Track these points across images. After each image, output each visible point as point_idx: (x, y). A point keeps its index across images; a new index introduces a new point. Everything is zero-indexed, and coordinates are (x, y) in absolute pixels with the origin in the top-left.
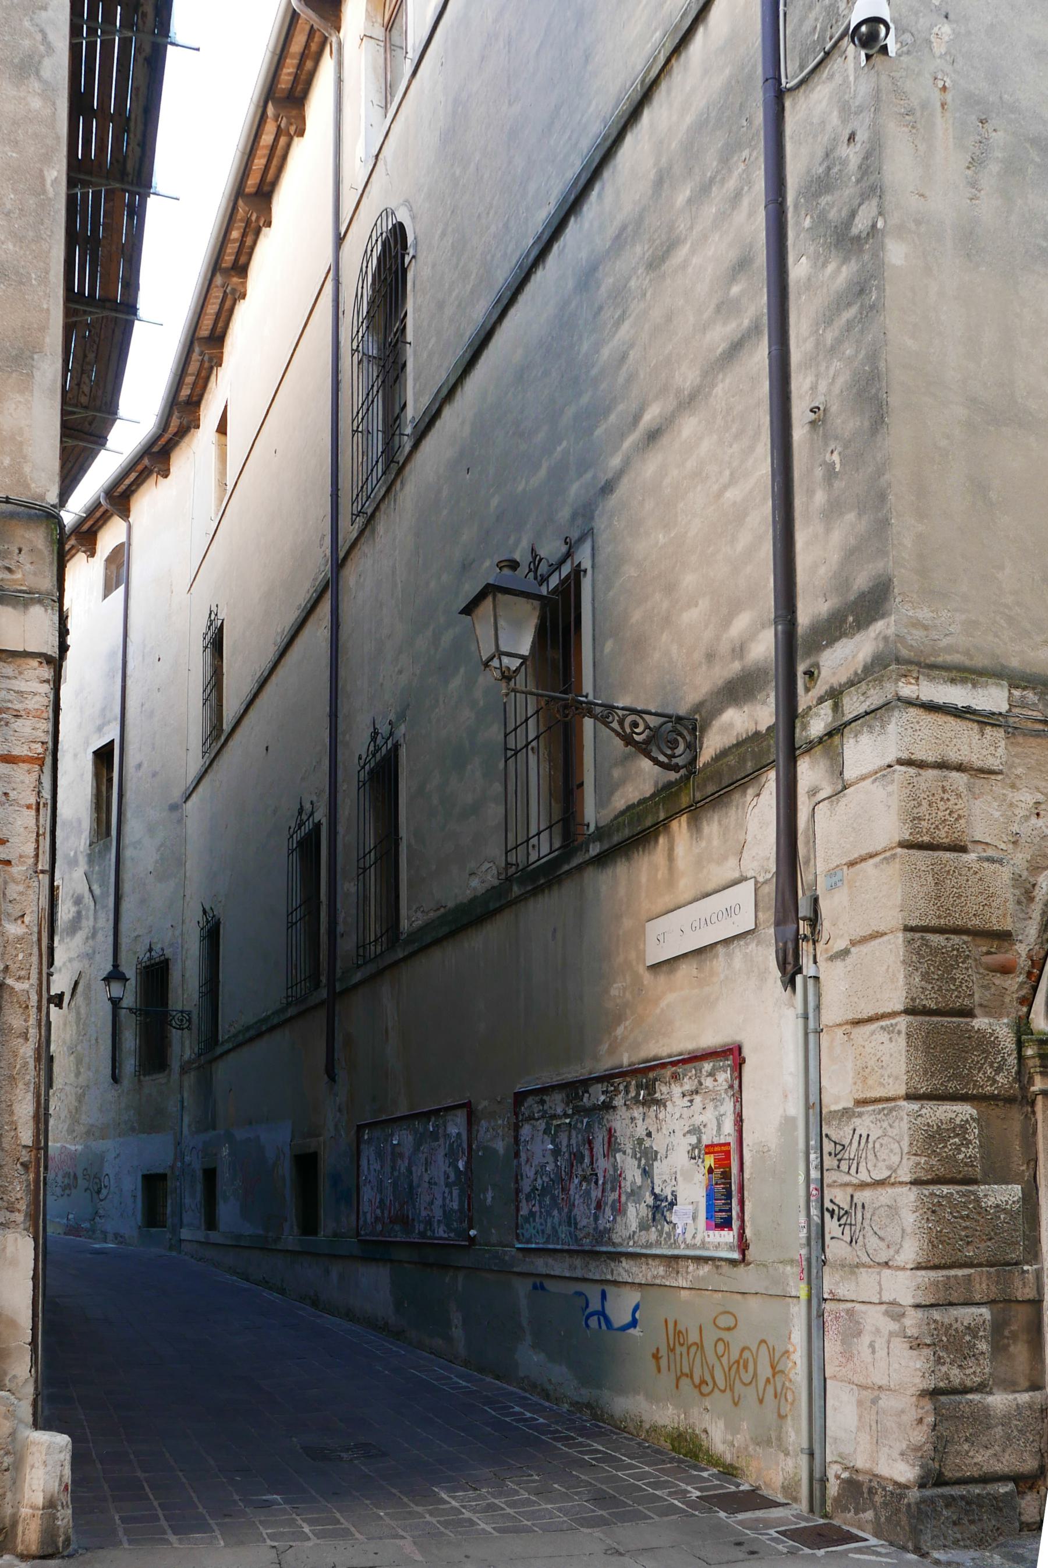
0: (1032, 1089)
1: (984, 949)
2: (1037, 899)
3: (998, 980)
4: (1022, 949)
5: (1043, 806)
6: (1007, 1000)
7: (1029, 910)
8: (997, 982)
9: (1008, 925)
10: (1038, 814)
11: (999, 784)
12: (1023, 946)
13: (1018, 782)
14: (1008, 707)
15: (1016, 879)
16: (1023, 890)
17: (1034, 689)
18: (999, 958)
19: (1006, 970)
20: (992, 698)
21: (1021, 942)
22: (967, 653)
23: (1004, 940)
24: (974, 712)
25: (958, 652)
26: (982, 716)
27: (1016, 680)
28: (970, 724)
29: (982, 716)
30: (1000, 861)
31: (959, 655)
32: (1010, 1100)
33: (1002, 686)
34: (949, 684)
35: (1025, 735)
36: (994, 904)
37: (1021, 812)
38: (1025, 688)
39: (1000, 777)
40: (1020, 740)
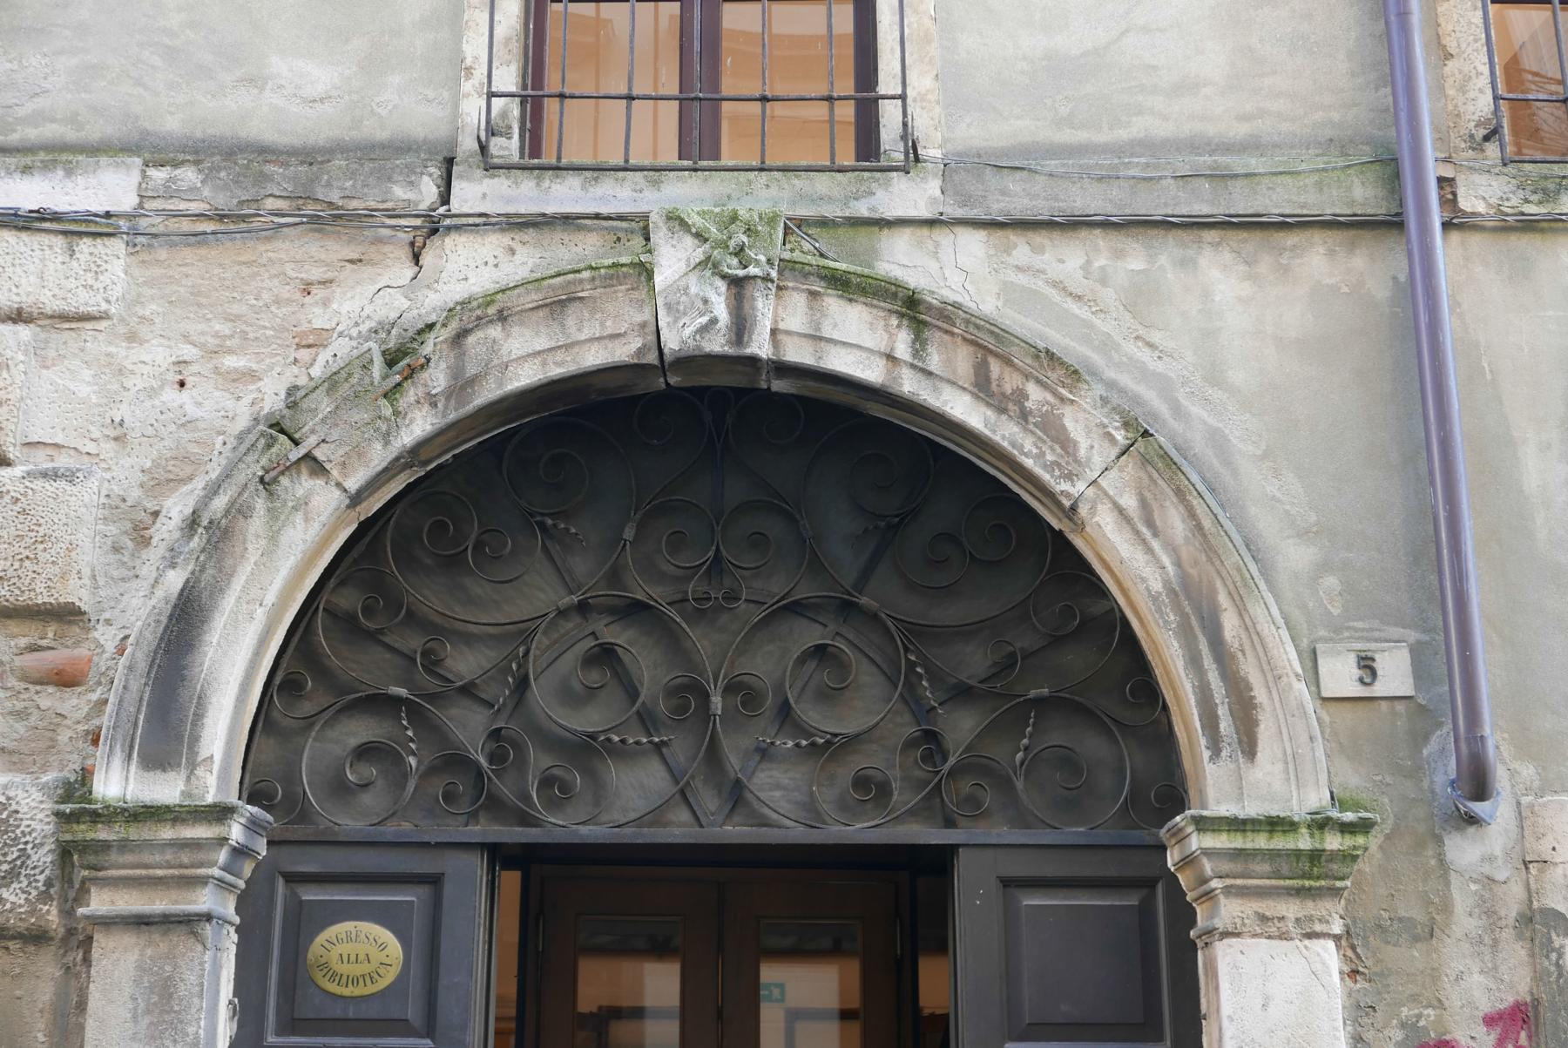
0: (81, 911)
1: (23, 642)
2: (154, 541)
3: (49, 699)
4: (107, 637)
5: (194, 368)
6: (64, 736)
7: (138, 562)
8: (45, 703)
9: (77, 593)
10: (182, 384)
11: (101, 337)
12: (112, 630)
13: (143, 330)
14: (137, 200)
15: (114, 508)
16: (129, 525)
17: (197, 163)
18: (58, 657)
19: (66, 680)
20: (110, 188)
21: (108, 622)
22: (73, 120)
23: (70, 622)
24: (56, 217)
25: (53, 120)
26: (75, 221)
27: (156, 152)
28: (46, 239)
29: (75, 221)
30: (70, 476)
31: (54, 126)
32: (37, 938)
33: (128, 167)
34: (17, 176)
35: (173, 245)
36: (42, 557)
37: (136, 383)
38: (176, 164)
39: (102, 325)
40: (162, 254)
